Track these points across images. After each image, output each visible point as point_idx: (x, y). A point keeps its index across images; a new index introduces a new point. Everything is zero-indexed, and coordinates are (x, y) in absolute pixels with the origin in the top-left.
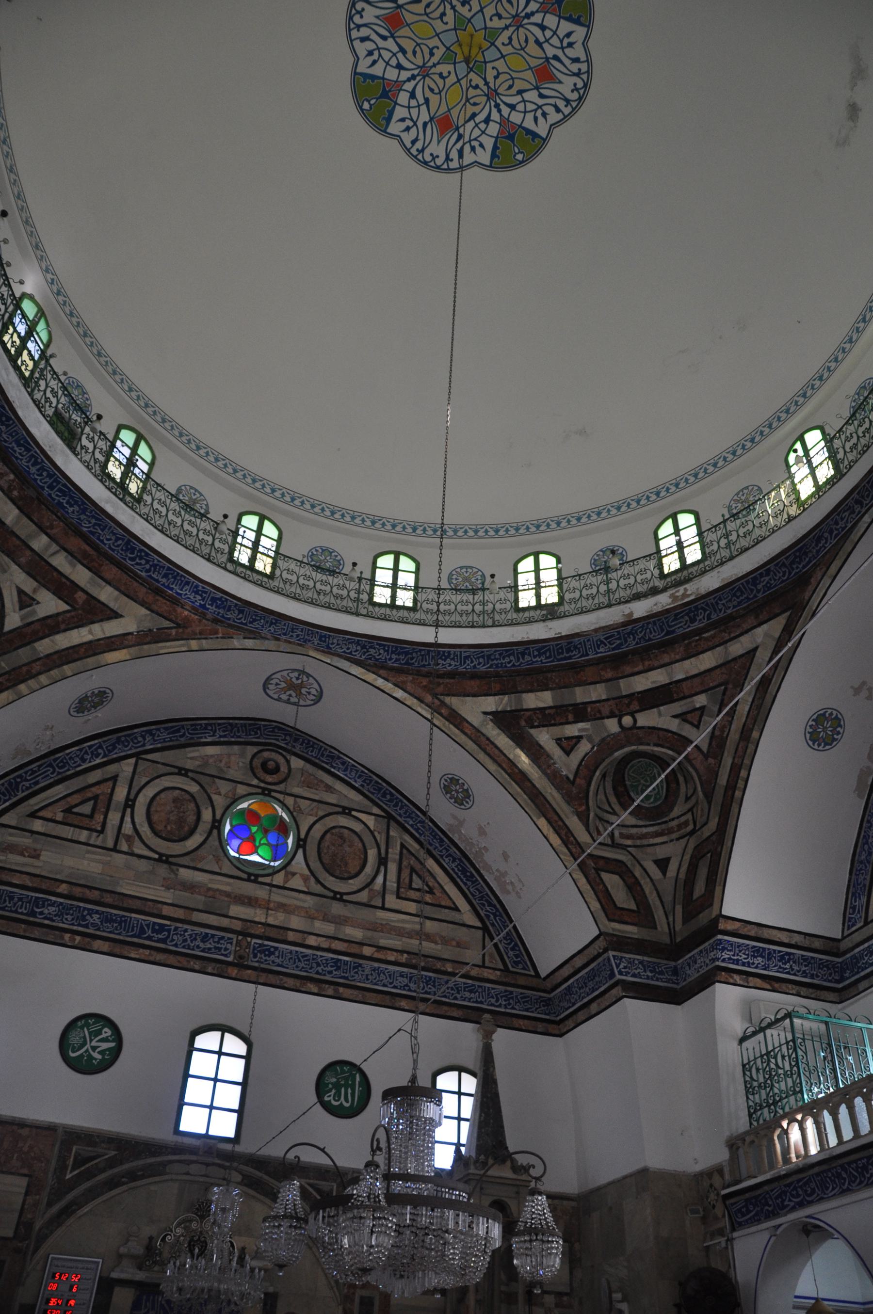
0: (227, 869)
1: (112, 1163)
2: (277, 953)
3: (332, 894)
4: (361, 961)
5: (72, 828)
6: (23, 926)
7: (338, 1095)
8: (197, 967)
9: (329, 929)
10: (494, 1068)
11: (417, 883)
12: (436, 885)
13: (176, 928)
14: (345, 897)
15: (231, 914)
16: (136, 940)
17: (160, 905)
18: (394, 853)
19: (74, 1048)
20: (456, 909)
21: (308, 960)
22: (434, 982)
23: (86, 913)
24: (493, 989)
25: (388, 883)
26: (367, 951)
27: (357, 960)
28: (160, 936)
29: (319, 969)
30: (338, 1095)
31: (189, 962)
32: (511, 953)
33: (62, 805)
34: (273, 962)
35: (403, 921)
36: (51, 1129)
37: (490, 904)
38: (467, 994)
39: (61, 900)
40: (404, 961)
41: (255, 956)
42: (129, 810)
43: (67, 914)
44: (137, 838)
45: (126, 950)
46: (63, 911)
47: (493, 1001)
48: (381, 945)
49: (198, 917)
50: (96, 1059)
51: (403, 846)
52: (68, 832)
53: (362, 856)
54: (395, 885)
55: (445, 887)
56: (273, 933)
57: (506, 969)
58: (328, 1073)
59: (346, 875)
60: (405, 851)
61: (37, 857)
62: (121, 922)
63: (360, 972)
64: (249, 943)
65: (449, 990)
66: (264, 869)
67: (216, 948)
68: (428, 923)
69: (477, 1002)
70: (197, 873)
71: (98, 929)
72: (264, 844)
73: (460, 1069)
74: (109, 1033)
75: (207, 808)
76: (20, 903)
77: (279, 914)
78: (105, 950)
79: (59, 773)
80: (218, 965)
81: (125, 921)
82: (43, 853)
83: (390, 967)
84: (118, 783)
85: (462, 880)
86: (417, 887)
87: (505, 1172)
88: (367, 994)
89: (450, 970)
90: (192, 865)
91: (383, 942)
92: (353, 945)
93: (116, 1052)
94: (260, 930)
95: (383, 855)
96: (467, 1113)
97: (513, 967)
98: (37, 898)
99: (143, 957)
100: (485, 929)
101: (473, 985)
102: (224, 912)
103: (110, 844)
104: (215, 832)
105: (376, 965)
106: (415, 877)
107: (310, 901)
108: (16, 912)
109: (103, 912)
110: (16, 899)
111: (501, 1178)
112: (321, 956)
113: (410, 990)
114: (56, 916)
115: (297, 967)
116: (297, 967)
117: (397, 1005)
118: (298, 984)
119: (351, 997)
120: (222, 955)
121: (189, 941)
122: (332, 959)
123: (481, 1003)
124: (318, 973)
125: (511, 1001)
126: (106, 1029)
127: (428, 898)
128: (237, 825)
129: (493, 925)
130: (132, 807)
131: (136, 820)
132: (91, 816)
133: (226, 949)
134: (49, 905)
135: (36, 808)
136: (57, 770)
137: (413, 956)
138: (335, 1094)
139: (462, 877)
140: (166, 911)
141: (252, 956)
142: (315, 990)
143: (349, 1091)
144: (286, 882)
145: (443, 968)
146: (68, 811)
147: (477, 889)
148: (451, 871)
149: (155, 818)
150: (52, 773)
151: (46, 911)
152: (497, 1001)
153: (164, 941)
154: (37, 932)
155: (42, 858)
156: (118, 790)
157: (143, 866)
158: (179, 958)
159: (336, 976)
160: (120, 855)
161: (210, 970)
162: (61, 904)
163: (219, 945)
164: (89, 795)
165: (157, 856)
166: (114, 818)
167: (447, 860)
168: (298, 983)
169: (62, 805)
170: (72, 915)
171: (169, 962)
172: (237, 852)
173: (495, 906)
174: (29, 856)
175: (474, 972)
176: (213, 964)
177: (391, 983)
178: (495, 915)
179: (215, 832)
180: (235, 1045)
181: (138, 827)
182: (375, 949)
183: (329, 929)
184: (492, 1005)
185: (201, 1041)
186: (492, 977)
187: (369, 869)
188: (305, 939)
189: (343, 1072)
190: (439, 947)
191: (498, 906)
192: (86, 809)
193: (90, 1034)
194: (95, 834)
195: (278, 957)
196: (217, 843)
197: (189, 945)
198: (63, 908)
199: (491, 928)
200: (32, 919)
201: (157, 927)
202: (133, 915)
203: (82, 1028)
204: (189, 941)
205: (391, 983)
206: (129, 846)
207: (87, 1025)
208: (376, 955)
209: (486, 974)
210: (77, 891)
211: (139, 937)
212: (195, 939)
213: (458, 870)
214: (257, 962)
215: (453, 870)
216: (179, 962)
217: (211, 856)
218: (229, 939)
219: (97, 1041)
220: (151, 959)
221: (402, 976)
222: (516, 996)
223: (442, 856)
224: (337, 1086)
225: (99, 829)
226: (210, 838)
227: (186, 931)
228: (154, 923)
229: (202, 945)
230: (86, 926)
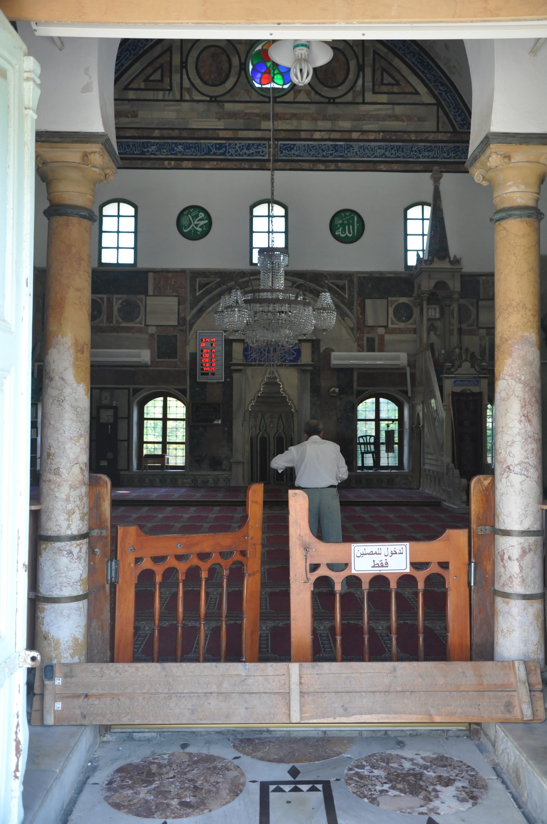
0: (255, 97)
1: (219, 285)
2: (295, 148)
3: (327, 100)
4: (351, 143)
5: (152, 92)
6: (139, 162)
7: (344, 231)
8: (247, 167)
9: (328, 125)
10: (440, 201)
11: (387, 79)
12: (401, 78)
13: (230, 144)
14: (336, 101)
15: (263, 127)
16: (207, 157)
17: (217, 131)
18: (369, 60)
19: (185, 227)
20: (417, 93)
21: (316, 149)
22: (403, 149)
23: (173, 146)
24: (445, 147)
25: (366, 84)
26: (355, 135)
27: (348, 143)
28: (221, 151)
29: (324, 153)
30: (344, 231)
31: (241, 164)
32: (458, 119)
33: (142, 77)
34: (294, 154)
35: (378, 110)
36: (183, 271)
37: (442, 84)
38: (427, 154)
39: (157, 141)
40: (381, 138)
41: (282, 153)
42: (184, 70)
43: (163, 149)
44: (194, 89)
45: (202, 164)
46: (160, 147)
47: (445, 155)
48: (364, 129)
49: (242, 134)
50: (199, 231)
51: (375, 53)
52: (150, 95)
53: (346, 68)
54: (371, 84)
55: (409, 78)
56: (291, 136)
57: (455, 131)
58: (336, 218)
59: (335, 84)
60: (377, 56)
61: (136, 116)
62: (195, 147)
63: (351, 151)
64: (277, 145)
65: (414, 153)
66: (279, 92)
67: (256, 152)
68: (396, 107)
69: (434, 158)
70: (236, 104)
71: (183, 155)
72: (277, 74)
73: (423, 204)
74: (203, 215)
75: (234, 56)
76: (134, 148)
77: (294, 121)
78: (190, 166)
79: (134, 54)
80: (260, 163)
81: (198, 146)
82: (139, 112)
83: (372, 144)
84: (173, 52)
85: (420, 70)
86: (387, 82)
87: (446, 265)
88: (357, 164)
89: (413, 138)
90: (232, 99)
91: (366, 127)
92: (345, 133)
93: (209, 225)
94: (283, 135)
95: (361, 63)
96: (426, 232)
97: (460, 128)
98: (143, 143)
99: (213, 167)
100: (439, 104)
101: (430, 146)
102: (258, 127)
103: (178, 98)
104: (243, 73)
105: (362, 144)
106: (385, 74)
107: (312, 108)
108: (133, 154)
109: (183, 143)
110: (131, 146)
111: (442, 268)
112: (324, 145)
113: (386, 157)
114: (156, 151)
115: (309, 155)
116: (309, 155)
117: (378, 168)
118: (311, 166)
119: (347, 169)
120: (261, 156)
121: (239, 151)
122: (332, 145)
123: (437, 157)
124: (323, 156)
125: (458, 153)
126: (201, 213)
127: (396, 89)
128: (257, 64)
129: (445, 100)
130: (186, 67)
131: (190, 76)
132: (162, 81)
133: (263, 152)
134: (151, 146)
135: (127, 83)
136: (132, 52)
137: (386, 133)
138: (342, 230)
139: (420, 67)
140: (222, 134)
141: (279, 153)
142: (323, 168)
143: (351, 227)
144: (295, 97)
145: (408, 138)
146: (146, 80)
147: (432, 75)
148: (412, 65)
149: (202, 72)
150: (130, 55)
151: (150, 150)
152: (448, 155)
153: (224, 154)
154: (148, 164)
155: (139, 116)
156: (174, 57)
157: (201, 107)
158: (235, 163)
159: (335, 157)
160: (186, 103)
161: (255, 167)
162: (158, 143)
163: (258, 150)
164: (158, 65)
165: (208, 99)
166: (176, 78)
167: (409, 56)
168: (311, 165)
169: (142, 77)
170: (166, 149)
171: (229, 167)
172: (260, 84)
173: (446, 85)
174: (132, 117)
175: (431, 137)
176: (257, 163)
177: (373, 155)
178: (446, 92)
179: (243, 73)
180: (278, 210)
181: (193, 81)
182: (360, 133)
183: (328, 125)
184: (445, 158)
185: (257, 211)
186: (445, 138)
187: (351, 76)
188: (312, 135)
189: (346, 216)
190: (405, 123)
191: (448, 84)
192: (157, 76)
193: (192, 217)
194: (167, 92)
195: (297, 150)
196: (245, 81)
197: (239, 154)
198: (160, 145)
199: (443, 102)
200: (143, 156)
201: (218, 146)
202: (202, 141)
203: (187, 215)
204: (239, 151)
205: (373, 155)
206: (190, 96)
207: (190, 213)
208: (362, 137)
209: (440, 137)
210: (165, 133)
211: (208, 154)
212: (243, 149)
213: (418, 62)
214: (284, 156)
215: (414, 63)
216: (235, 165)
217: (243, 91)
218: (264, 144)
219: (198, 221)
220: (219, 166)
221: (380, 148)
222: (462, 149)
223: (404, 54)
224: (343, 225)
225: (169, 88)
226: (241, 78)
227: (236, 144)
228: (216, 144)
229: (247, 152)
230: (176, 154)
